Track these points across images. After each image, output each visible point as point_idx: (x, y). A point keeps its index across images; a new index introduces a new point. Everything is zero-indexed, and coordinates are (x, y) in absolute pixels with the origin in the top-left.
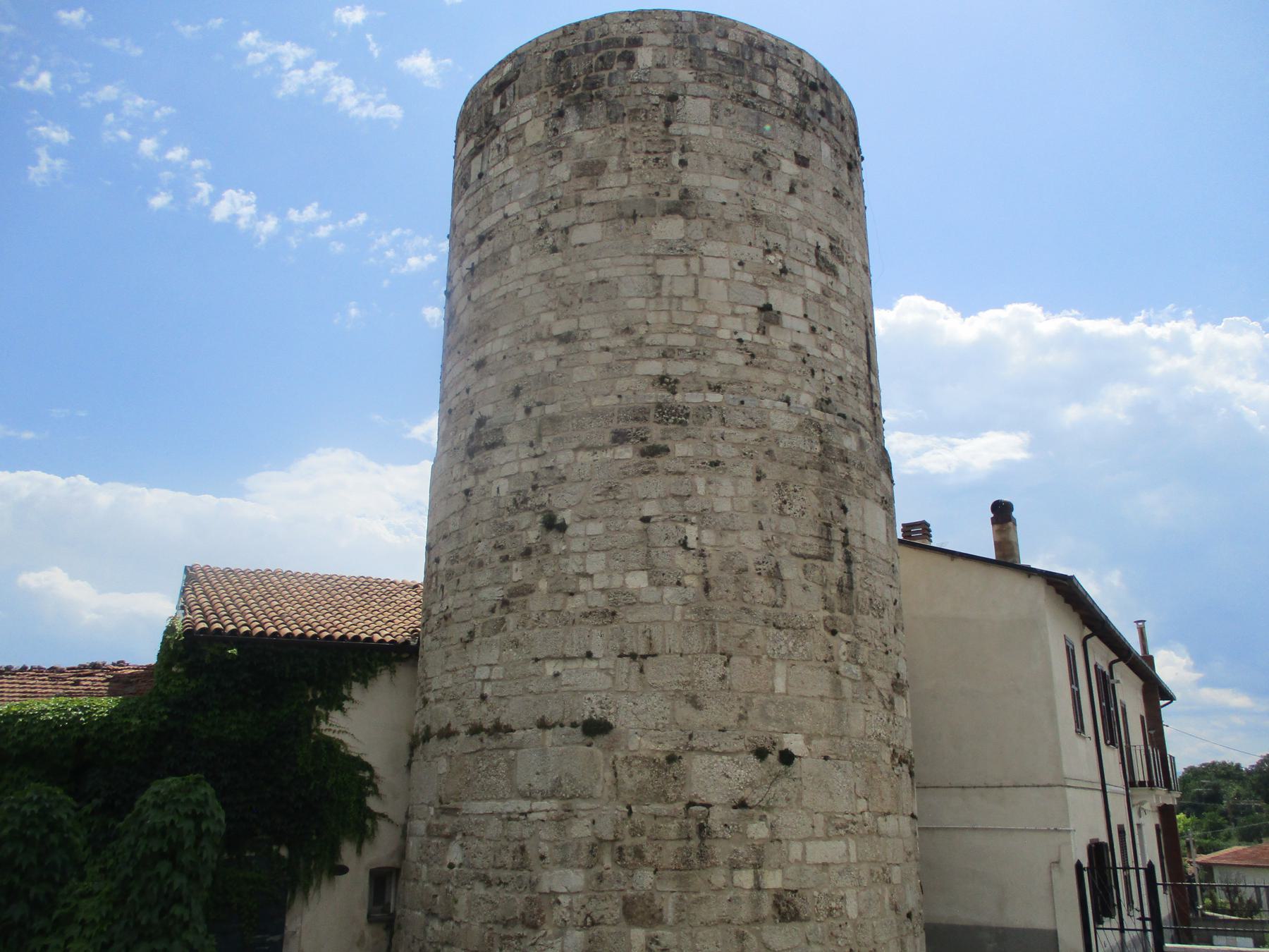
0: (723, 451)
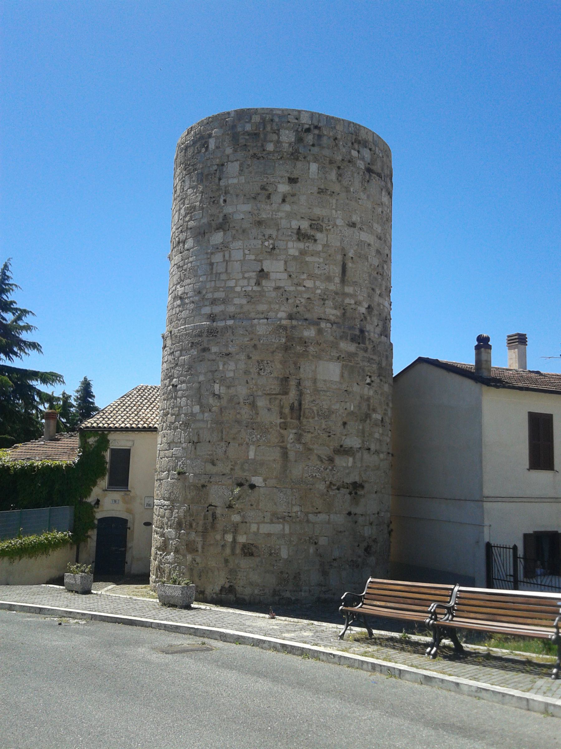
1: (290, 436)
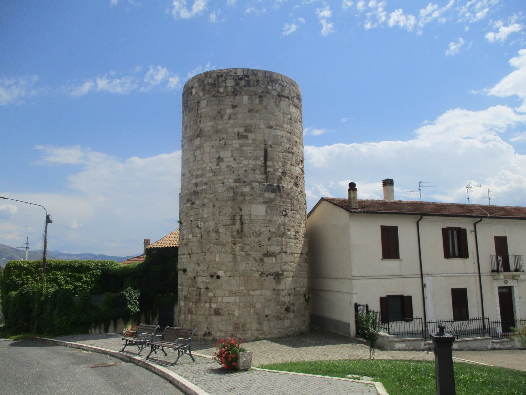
0: (206, 201)
1: (237, 248)
